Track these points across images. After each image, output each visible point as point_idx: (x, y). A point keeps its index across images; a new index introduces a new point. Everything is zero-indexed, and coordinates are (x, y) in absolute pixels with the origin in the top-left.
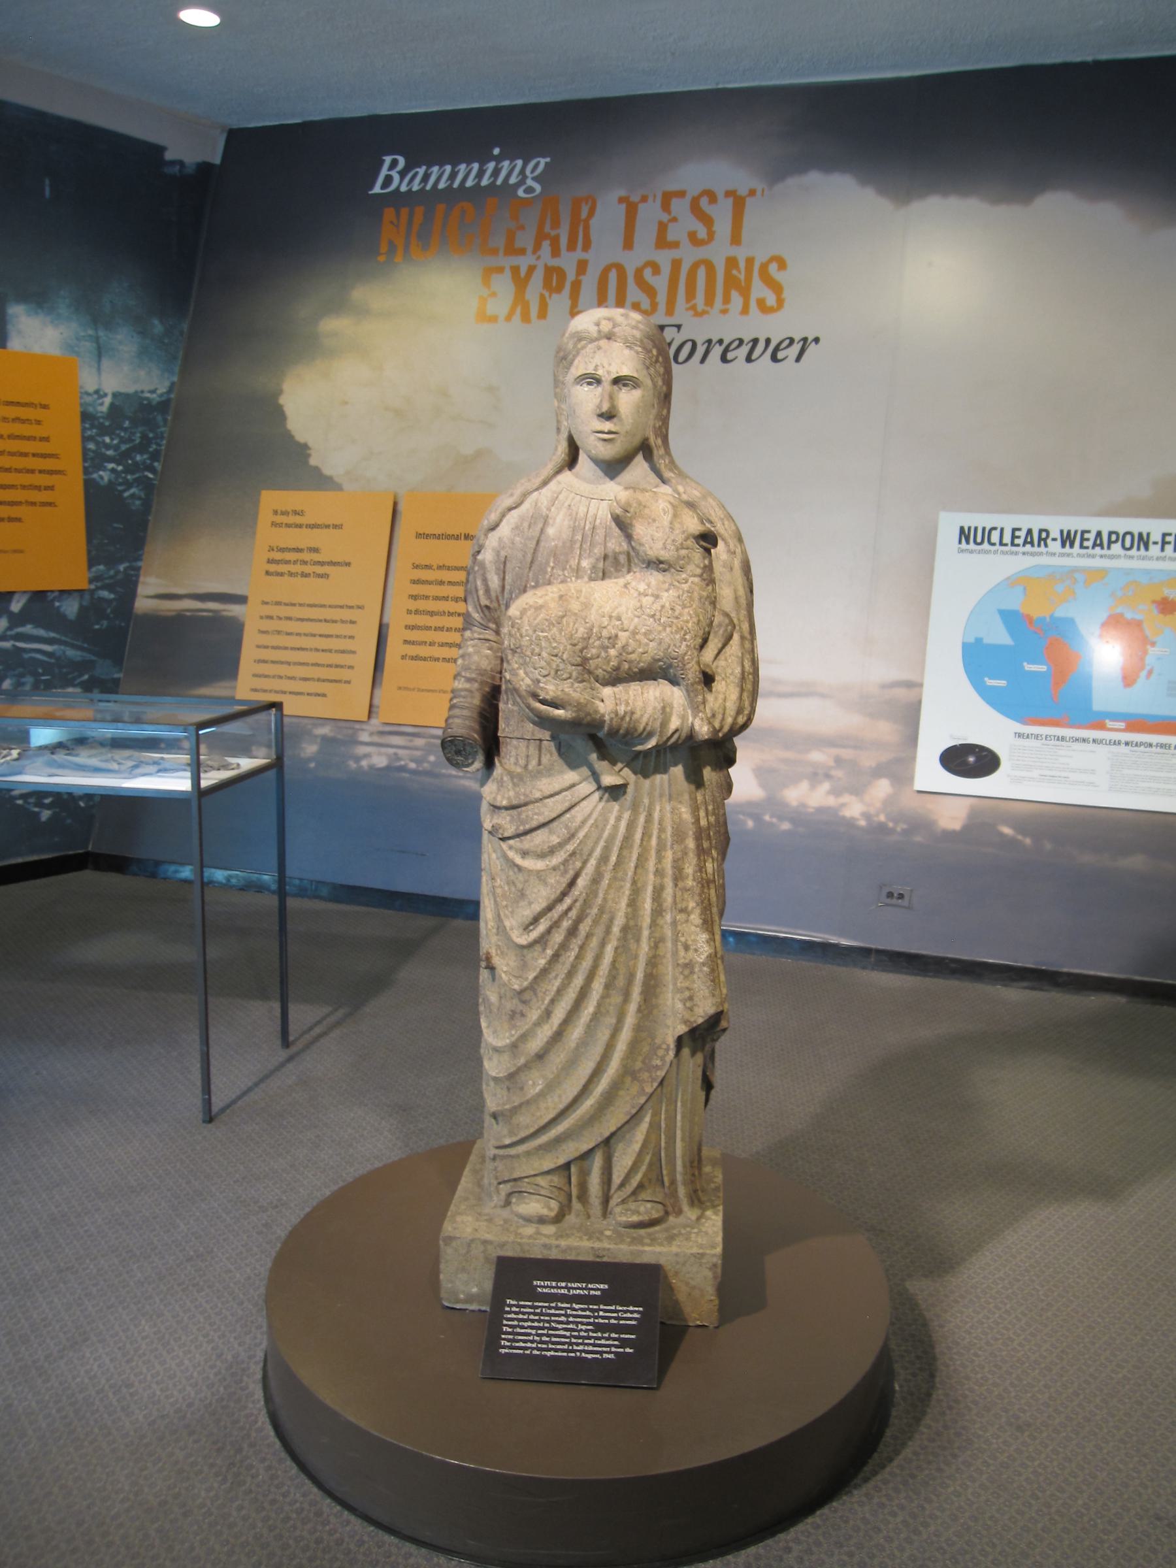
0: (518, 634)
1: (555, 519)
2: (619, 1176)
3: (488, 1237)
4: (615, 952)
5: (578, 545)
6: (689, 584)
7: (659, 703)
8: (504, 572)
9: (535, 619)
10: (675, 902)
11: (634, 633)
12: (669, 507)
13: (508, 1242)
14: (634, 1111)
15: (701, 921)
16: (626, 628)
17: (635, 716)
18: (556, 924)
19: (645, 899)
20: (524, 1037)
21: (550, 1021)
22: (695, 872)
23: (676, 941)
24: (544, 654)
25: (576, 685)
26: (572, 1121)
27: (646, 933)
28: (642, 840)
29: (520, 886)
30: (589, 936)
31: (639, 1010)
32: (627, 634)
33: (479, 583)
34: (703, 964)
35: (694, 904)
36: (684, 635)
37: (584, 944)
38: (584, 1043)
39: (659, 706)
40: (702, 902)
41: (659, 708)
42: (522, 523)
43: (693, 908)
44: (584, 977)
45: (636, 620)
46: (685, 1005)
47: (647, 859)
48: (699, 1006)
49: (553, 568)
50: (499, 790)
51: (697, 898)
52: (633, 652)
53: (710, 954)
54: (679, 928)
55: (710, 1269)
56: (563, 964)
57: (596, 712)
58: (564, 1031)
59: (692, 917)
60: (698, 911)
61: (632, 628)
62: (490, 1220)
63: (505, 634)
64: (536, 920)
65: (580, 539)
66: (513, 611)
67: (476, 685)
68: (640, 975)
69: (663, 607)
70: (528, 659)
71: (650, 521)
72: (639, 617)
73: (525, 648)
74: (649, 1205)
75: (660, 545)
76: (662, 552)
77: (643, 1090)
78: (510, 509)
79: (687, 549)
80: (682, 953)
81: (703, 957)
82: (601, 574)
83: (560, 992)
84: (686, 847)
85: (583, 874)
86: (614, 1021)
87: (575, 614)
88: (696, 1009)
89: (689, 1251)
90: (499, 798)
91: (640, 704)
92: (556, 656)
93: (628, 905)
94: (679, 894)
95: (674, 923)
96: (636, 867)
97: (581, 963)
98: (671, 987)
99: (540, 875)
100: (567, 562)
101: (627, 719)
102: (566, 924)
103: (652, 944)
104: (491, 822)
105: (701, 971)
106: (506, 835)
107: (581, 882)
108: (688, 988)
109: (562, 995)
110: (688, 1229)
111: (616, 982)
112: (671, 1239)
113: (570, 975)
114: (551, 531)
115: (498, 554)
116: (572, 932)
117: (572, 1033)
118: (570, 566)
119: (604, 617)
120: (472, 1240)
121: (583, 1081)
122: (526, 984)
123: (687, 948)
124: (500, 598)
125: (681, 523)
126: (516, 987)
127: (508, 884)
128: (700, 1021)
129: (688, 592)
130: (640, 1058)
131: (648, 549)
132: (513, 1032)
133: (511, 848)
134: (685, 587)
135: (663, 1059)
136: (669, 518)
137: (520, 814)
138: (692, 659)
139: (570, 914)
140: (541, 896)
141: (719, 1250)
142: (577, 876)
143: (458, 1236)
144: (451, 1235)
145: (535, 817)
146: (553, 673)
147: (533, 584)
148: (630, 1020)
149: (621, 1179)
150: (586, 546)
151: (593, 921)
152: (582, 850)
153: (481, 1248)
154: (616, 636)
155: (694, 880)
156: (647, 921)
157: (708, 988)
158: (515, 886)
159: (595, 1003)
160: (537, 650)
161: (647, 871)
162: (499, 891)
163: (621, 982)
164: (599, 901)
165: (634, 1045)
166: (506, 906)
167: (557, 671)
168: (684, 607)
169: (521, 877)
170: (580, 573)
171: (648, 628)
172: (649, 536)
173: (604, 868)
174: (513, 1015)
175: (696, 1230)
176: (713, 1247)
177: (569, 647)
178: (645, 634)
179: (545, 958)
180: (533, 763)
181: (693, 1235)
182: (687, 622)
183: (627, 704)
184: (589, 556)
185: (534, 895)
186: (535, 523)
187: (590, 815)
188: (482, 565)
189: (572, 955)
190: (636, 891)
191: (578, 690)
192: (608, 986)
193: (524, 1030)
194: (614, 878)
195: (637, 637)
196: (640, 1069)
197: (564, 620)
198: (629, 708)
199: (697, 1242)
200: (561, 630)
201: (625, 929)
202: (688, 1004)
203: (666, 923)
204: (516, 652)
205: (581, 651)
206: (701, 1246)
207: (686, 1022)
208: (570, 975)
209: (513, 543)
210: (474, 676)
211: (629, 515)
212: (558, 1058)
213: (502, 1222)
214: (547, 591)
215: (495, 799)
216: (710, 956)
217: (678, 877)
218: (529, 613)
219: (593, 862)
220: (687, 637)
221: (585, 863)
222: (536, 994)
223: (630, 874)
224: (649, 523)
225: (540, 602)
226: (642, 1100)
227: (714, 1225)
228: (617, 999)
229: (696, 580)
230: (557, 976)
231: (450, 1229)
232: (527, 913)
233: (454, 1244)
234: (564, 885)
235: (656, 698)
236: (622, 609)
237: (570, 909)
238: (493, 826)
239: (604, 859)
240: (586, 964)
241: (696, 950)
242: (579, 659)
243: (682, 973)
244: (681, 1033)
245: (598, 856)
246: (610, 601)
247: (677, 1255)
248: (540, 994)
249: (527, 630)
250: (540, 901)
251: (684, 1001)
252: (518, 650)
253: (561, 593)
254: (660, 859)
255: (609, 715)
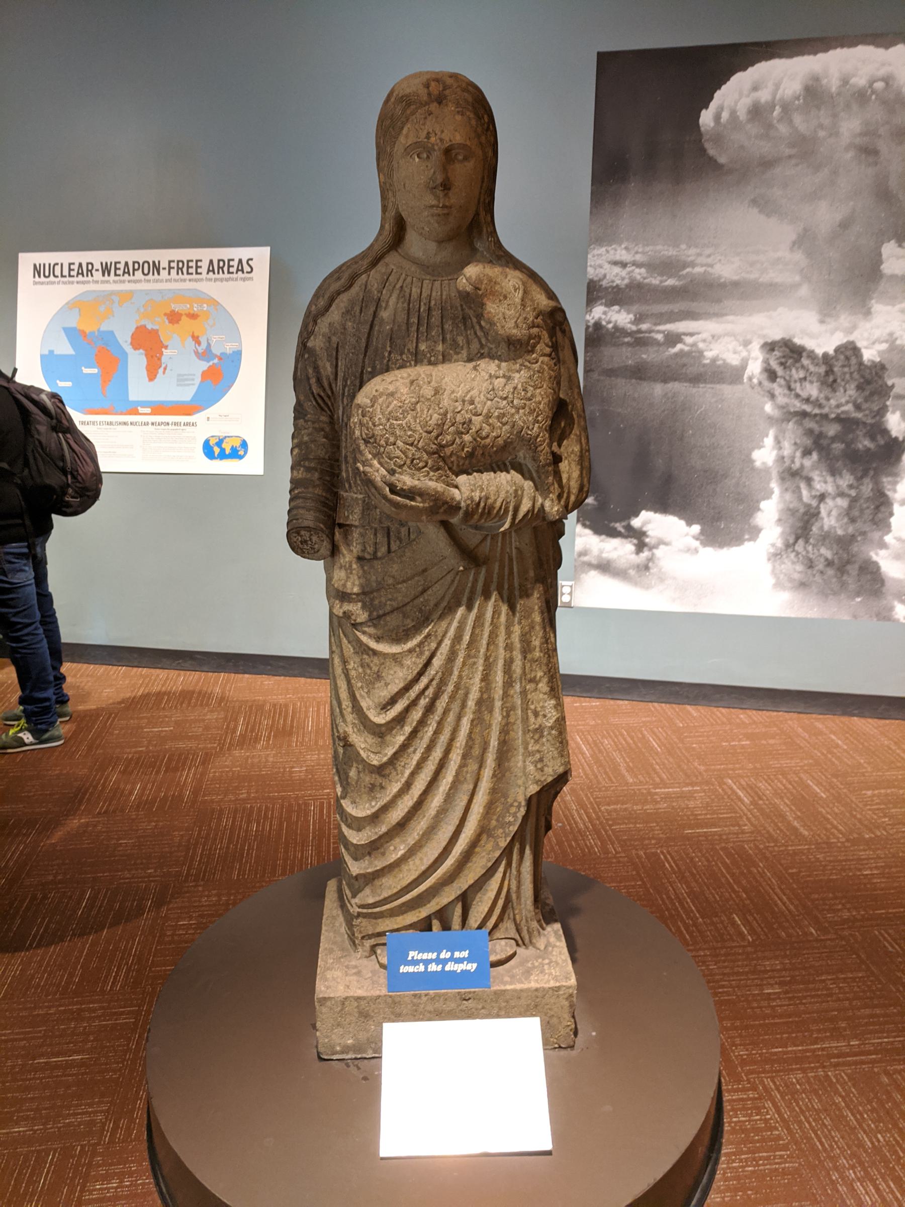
0: (370, 423)
1: (388, 302)
2: (476, 921)
3: (360, 993)
4: (471, 725)
5: (414, 328)
6: (539, 363)
7: (511, 487)
8: (337, 359)
9: (388, 407)
10: (524, 673)
11: (488, 416)
12: (520, 283)
13: (379, 996)
14: (490, 864)
15: (548, 689)
16: (479, 412)
17: (490, 501)
18: (414, 703)
19: (496, 672)
20: (385, 809)
21: (410, 792)
22: (542, 644)
23: (525, 710)
24: (399, 443)
25: (432, 474)
26: (433, 881)
27: (498, 704)
28: (493, 618)
29: (375, 669)
30: (446, 712)
31: (494, 775)
32: (481, 418)
33: (310, 371)
34: (552, 728)
35: (542, 674)
36: (537, 417)
37: (442, 719)
38: (442, 811)
39: (512, 490)
40: (549, 671)
41: (511, 491)
42: (353, 308)
43: (541, 677)
44: (442, 750)
45: (489, 403)
46: (536, 766)
47: (497, 636)
48: (548, 767)
49: (390, 353)
50: (348, 577)
51: (544, 668)
52: (488, 436)
53: (558, 718)
54: (529, 696)
55: (567, 999)
56: (421, 739)
57: (453, 499)
58: (425, 799)
59: (540, 685)
60: (545, 680)
61: (485, 411)
62: (358, 973)
63: (355, 424)
64: (393, 701)
65: (416, 321)
66: (362, 398)
67: (316, 475)
68: (494, 743)
69: (515, 388)
70: (382, 449)
71: (502, 298)
72: (492, 400)
73: (378, 438)
74: (503, 942)
75: (511, 324)
76: (515, 331)
77: (497, 844)
78: (339, 293)
79: (538, 327)
80: (532, 719)
81: (552, 721)
82: (441, 357)
83: (419, 767)
84: (533, 621)
85: (438, 654)
86: (471, 787)
87: (429, 400)
88: (546, 769)
89: (547, 986)
90: (349, 584)
91: (492, 489)
92: (412, 445)
93: (482, 680)
94: (528, 665)
95: (524, 693)
96: (488, 644)
97: (439, 738)
98: (521, 750)
99: (396, 659)
100: (405, 346)
101: (482, 504)
102: (423, 702)
103: (505, 714)
104: (341, 607)
105: (549, 734)
106: (359, 620)
107: (437, 662)
108: (538, 751)
109: (422, 768)
110: (540, 960)
111: (473, 751)
112: (528, 973)
113: (429, 748)
114: (385, 314)
115: (329, 340)
116: (430, 709)
117: (432, 801)
118: (409, 350)
119: (457, 401)
120: (346, 998)
121: (444, 844)
122: (385, 759)
123: (536, 714)
124: (334, 385)
125: (533, 300)
126: (375, 763)
127: (362, 666)
128: (550, 779)
129: (539, 372)
130: (495, 817)
131: (499, 328)
132: (373, 804)
133: (364, 633)
134: (536, 367)
135: (515, 815)
136: (520, 295)
137: (372, 600)
138: (544, 441)
139: (427, 693)
140: (397, 678)
141: (573, 981)
142: (433, 655)
143: (332, 995)
144: (326, 996)
145: (388, 602)
146: (408, 462)
147: (369, 369)
148: (485, 785)
149: (478, 923)
150: (423, 329)
151: (450, 697)
152: (436, 631)
153: (356, 1004)
154: (470, 421)
155: (541, 651)
156: (498, 693)
157: (557, 749)
158: (371, 669)
159: (454, 773)
160: (392, 439)
161: (497, 646)
162: (353, 673)
163: (476, 751)
164: (455, 677)
165: (489, 807)
166: (362, 687)
167: (413, 460)
168: (535, 387)
169: (376, 660)
170: (419, 357)
171: (502, 411)
172: (501, 315)
173: (458, 647)
174: (372, 788)
175: (547, 961)
176: (567, 978)
177: (424, 434)
178: (498, 418)
179: (404, 734)
180: (383, 550)
181: (546, 967)
182: (540, 403)
183: (482, 490)
184: (427, 339)
185: (390, 677)
186: (366, 306)
187: (444, 597)
188: (311, 352)
189: (430, 730)
190: (489, 666)
191: (434, 478)
192: (465, 756)
193: (385, 801)
194: (468, 657)
195: (491, 421)
196: (495, 827)
197: (418, 406)
198: (483, 494)
199: (551, 974)
200: (415, 418)
201: (479, 702)
202: (539, 766)
203: (516, 693)
204: (369, 442)
205: (436, 438)
206: (556, 979)
207: (537, 782)
208: (429, 748)
209: (345, 329)
210: (312, 465)
211: (480, 293)
212: (420, 825)
213: (370, 975)
214: (396, 376)
215: (344, 585)
216: (557, 720)
217: (526, 650)
218: (380, 400)
219: (447, 642)
220: (540, 418)
221: (439, 644)
222: (395, 769)
223: (483, 651)
224: (500, 301)
225: (391, 388)
226: (497, 854)
227: (560, 953)
228: (473, 766)
229: (546, 359)
230: (415, 750)
231: (323, 989)
232: (385, 694)
233: (329, 1003)
234: (420, 666)
235: (507, 482)
236: (474, 393)
237: (427, 688)
238: (344, 613)
239: (458, 638)
240: (444, 738)
241: (545, 716)
242: (434, 446)
243: (532, 738)
244: (533, 792)
245: (452, 637)
246: (462, 385)
247: (537, 990)
248: (399, 768)
249: (380, 419)
250: (397, 681)
251: (535, 763)
252: (372, 440)
253: (411, 378)
254: (509, 633)
255: (465, 501)
